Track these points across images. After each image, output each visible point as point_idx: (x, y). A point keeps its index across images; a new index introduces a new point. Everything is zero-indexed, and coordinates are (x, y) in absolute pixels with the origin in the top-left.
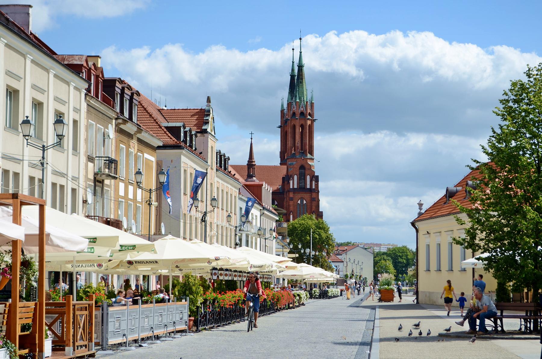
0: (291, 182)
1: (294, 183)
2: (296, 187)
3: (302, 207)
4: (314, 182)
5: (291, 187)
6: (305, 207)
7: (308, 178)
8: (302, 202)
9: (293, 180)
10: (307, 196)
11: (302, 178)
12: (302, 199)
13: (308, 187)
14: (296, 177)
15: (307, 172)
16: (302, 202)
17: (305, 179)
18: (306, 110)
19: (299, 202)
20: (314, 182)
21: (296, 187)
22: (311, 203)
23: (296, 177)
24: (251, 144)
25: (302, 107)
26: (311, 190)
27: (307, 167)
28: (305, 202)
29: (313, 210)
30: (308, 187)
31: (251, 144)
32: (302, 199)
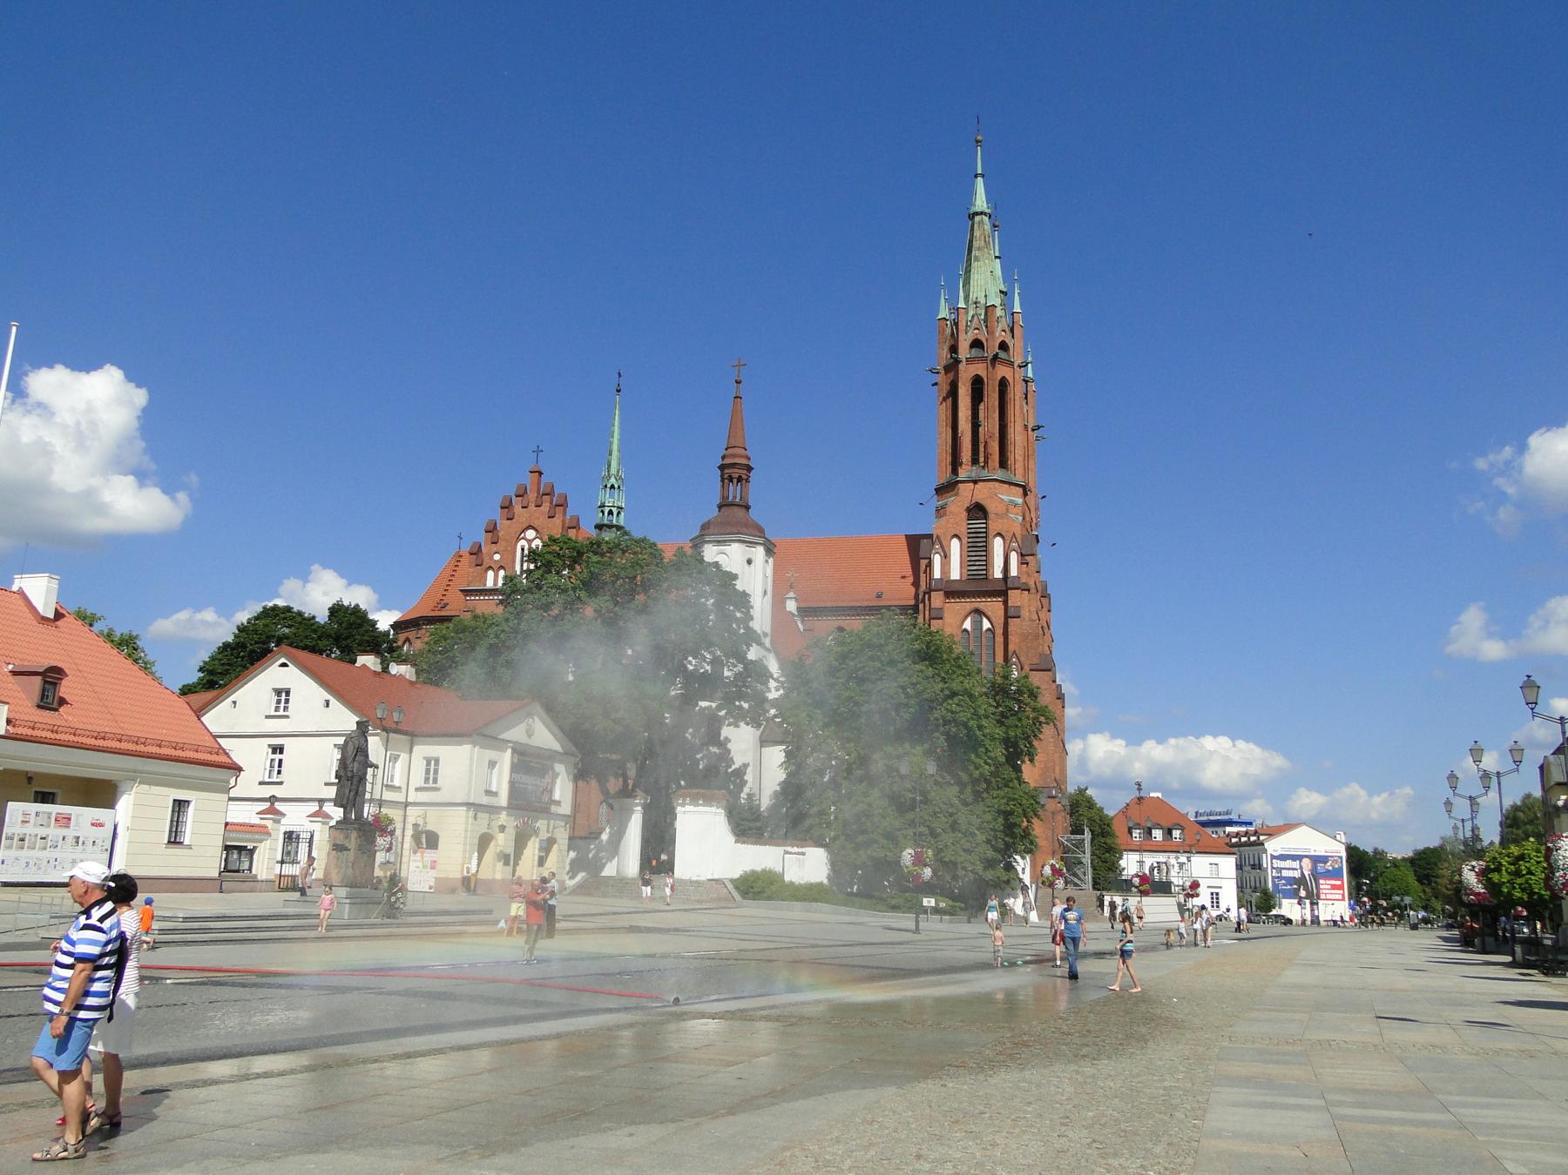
0: (937, 560)
1: (951, 564)
2: (955, 574)
4: (1014, 557)
5: (937, 574)
7: (998, 545)
9: (946, 557)
11: (978, 548)
13: (998, 574)
14: (955, 546)
15: (994, 525)
16: (977, 625)
17: (986, 549)
18: (990, 332)
19: (967, 625)
20: (1014, 557)
21: (955, 574)
23: (955, 546)
27: (991, 507)
28: (986, 625)
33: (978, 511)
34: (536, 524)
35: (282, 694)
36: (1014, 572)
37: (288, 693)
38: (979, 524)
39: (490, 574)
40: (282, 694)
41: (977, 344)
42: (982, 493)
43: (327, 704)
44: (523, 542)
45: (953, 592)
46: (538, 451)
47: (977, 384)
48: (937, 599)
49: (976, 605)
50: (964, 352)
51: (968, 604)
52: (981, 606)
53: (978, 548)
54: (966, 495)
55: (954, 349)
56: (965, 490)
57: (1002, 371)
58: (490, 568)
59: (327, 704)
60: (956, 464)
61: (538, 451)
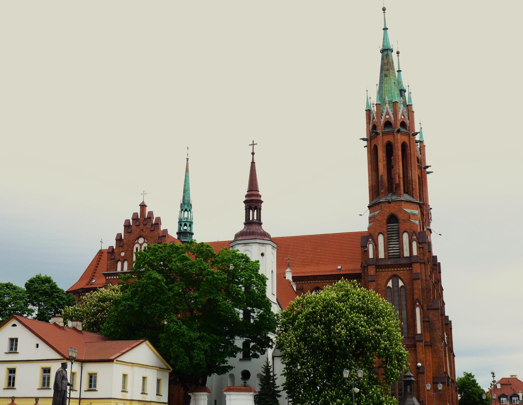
0: (371, 247)
3: (396, 294)
4: (414, 244)
5: (371, 256)
6: (403, 293)
8: (395, 284)
10: (402, 272)
13: (406, 254)
14: (381, 239)
15: (403, 227)
16: (395, 284)
19: (390, 284)
20: (414, 244)
21: (382, 255)
22: (413, 284)
23: (381, 239)
24: (253, 163)
25: (388, 114)
26: (410, 262)
27: (400, 216)
28: (401, 284)
29: (416, 297)
30: (406, 254)
31: (253, 163)
32: (395, 277)
33: (393, 219)
34: (144, 234)
35: (13, 342)
36: (415, 253)
37: (17, 340)
39: (119, 264)
40: (13, 342)
43: (37, 346)
44: (137, 245)
46: (144, 194)
49: (395, 273)
51: (390, 272)
52: (397, 273)
58: (119, 260)
59: (37, 346)
61: (144, 194)
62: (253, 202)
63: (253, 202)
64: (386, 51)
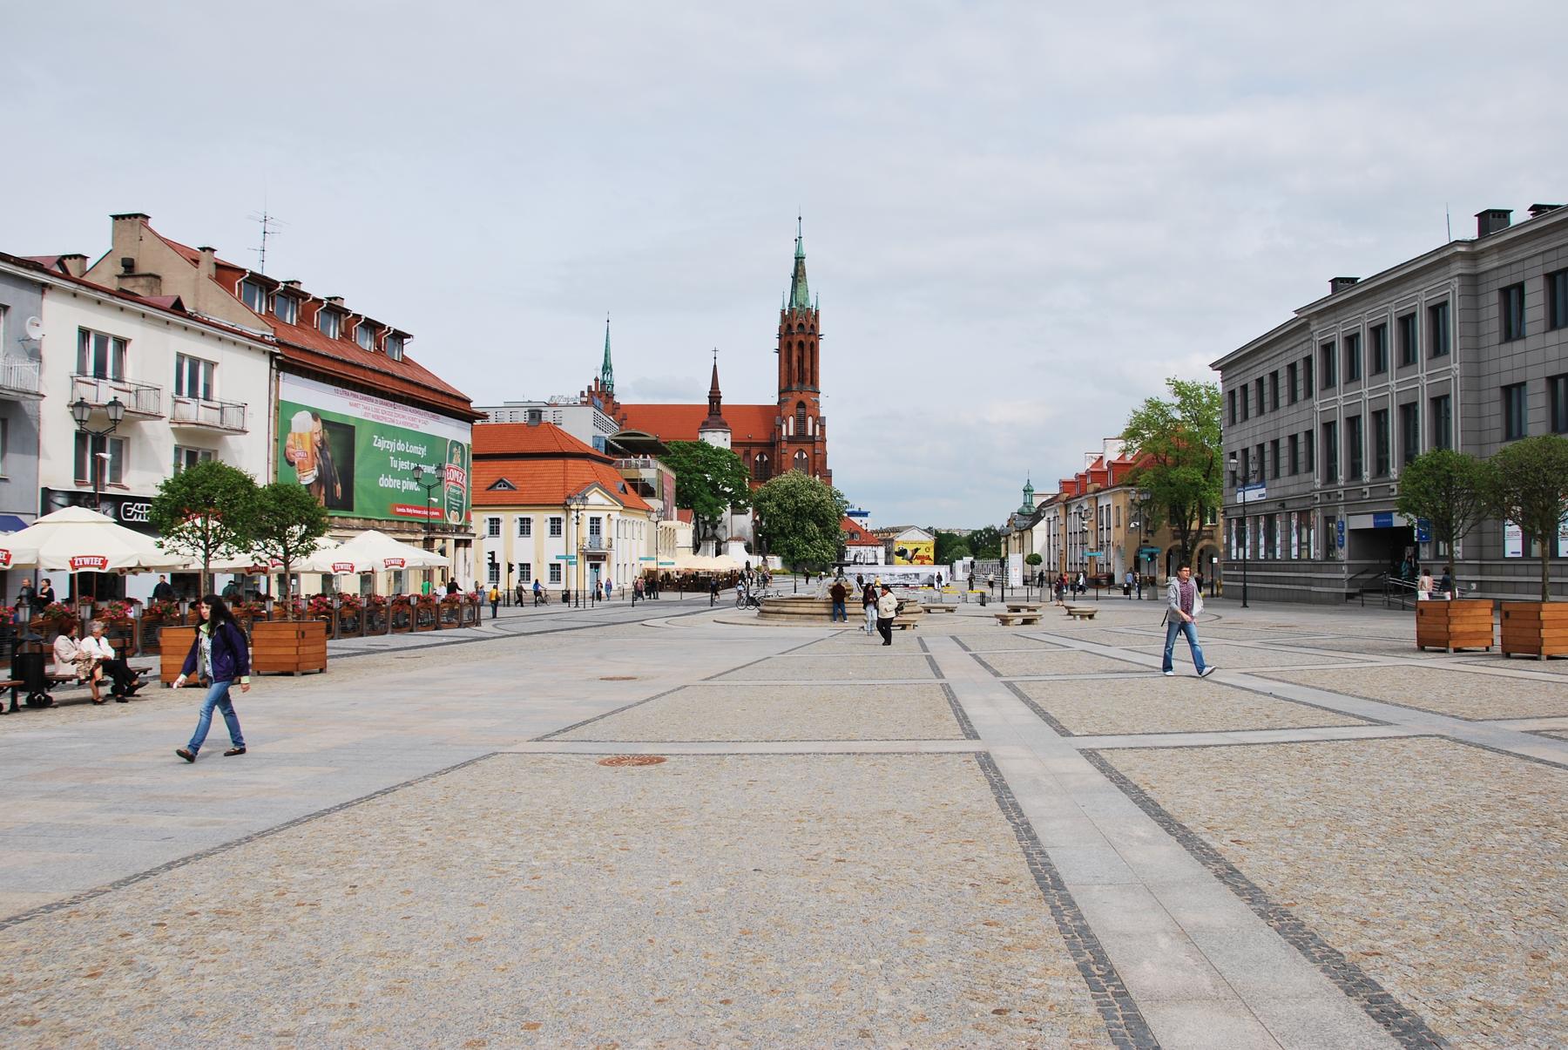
1: (789, 428)
7: (810, 420)
10: (808, 447)
11: (801, 422)
12: (801, 451)
17: (805, 422)
32: (801, 451)
33: (801, 405)
38: (801, 411)
41: (801, 325)
42: (803, 397)
45: (791, 440)
47: (801, 344)
48: (784, 445)
50: (795, 331)
51: (797, 447)
53: (801, 422)
54: (797, 397)
55: (790, 326)
56: (796, 394)
57: (812, 338)
60: (790, 384)
62: (715, 396)
63: (715, 396)
64: (799, 260)
